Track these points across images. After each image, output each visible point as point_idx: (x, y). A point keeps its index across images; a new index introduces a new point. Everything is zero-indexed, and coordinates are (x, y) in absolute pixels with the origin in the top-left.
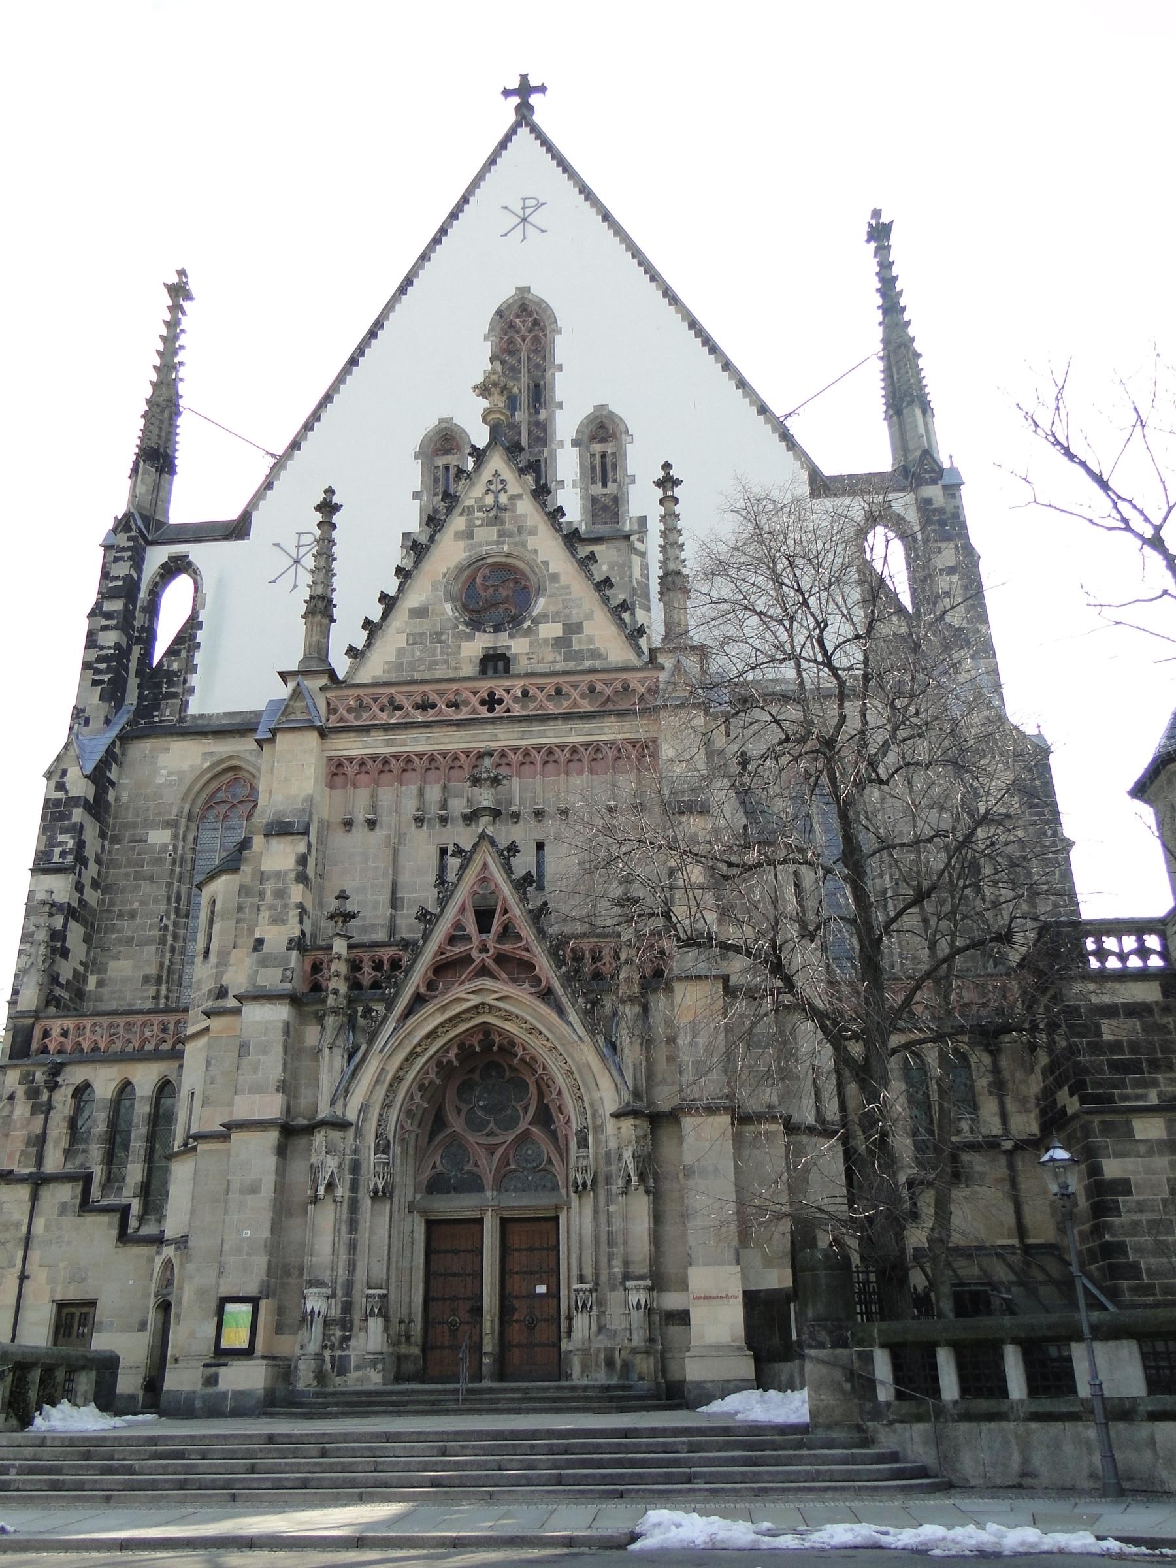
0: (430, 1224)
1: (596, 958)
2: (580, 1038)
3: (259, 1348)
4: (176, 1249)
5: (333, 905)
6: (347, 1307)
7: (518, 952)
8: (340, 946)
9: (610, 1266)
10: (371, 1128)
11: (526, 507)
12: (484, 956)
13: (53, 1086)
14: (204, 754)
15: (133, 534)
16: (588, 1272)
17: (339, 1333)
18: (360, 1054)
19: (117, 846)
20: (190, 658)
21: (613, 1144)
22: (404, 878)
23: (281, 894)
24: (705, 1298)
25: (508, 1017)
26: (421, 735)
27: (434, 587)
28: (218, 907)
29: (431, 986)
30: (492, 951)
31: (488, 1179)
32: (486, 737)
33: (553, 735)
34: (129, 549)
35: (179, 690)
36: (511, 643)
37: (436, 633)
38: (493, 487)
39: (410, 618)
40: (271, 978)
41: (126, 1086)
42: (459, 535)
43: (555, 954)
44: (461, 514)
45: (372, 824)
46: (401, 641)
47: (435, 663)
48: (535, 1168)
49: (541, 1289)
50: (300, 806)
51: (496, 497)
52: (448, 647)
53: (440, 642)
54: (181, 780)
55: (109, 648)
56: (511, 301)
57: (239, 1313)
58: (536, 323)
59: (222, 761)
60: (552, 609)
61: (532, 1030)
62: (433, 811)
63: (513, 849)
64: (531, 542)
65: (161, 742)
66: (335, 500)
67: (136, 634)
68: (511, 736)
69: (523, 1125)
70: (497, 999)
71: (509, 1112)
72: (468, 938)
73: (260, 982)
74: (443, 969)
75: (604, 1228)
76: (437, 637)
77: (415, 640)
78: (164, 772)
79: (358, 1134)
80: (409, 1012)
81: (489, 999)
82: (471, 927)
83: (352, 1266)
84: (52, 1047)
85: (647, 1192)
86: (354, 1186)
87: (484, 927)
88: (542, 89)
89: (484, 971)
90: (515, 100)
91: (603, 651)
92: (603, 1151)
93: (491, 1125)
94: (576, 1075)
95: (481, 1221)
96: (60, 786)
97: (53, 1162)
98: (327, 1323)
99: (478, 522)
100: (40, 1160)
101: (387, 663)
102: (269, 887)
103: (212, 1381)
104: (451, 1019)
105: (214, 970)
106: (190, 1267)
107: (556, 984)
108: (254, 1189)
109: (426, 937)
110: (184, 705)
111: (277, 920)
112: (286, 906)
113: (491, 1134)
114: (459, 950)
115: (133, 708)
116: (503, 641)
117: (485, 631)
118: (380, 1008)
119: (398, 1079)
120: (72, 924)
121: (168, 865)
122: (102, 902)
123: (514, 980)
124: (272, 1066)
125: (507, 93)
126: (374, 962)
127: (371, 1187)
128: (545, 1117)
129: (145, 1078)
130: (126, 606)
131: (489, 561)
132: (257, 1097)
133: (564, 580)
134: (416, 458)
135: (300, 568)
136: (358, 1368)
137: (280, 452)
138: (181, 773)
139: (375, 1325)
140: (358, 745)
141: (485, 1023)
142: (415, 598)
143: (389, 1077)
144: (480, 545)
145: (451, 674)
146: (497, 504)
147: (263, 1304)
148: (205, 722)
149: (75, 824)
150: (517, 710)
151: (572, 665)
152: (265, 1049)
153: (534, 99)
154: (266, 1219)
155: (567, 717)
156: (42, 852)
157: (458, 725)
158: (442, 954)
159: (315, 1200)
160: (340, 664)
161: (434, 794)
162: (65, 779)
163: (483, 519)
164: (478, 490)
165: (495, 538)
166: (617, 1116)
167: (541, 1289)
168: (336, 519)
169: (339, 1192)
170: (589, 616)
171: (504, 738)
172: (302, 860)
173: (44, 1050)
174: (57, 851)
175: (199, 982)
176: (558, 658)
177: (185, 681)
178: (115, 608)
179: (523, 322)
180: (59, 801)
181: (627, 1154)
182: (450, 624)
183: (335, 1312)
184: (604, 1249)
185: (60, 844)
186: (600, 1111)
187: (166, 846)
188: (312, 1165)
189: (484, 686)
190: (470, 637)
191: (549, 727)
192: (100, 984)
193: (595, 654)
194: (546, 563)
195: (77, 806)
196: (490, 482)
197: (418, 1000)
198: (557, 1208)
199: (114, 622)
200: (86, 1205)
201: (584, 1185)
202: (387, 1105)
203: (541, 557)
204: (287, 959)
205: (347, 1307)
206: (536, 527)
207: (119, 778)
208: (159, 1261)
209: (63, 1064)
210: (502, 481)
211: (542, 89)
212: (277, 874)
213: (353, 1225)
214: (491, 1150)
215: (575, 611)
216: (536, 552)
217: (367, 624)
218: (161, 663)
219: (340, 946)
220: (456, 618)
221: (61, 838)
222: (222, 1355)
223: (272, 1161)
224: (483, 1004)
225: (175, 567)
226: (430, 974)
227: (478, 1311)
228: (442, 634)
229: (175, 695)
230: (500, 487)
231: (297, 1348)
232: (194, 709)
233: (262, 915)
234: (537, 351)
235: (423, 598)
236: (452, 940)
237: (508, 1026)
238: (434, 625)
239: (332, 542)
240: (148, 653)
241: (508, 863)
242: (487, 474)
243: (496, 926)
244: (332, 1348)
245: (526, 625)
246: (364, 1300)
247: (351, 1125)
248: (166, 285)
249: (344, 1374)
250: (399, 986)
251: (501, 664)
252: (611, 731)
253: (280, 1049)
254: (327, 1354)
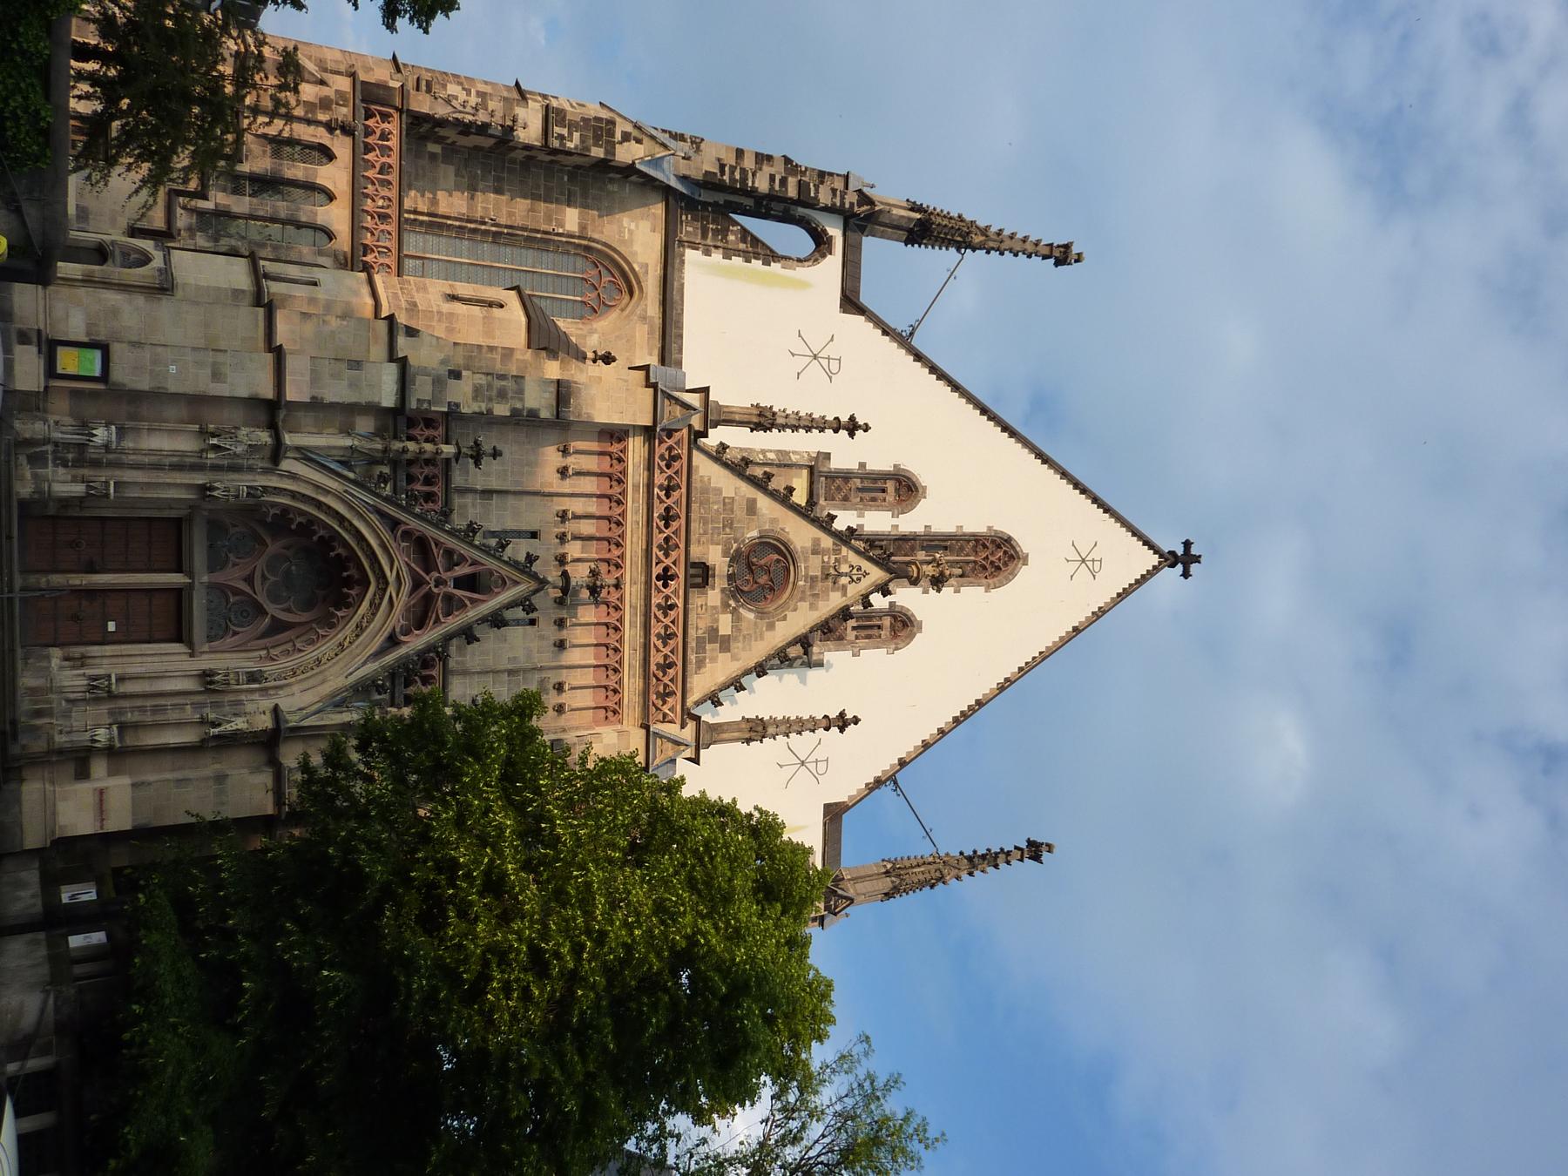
0: (178, 522)
1: (426, 680)
2: (351, 674)
4: (160, 270)
5: (487, 447)
7: (434, 615)
8: (448, 450)
9: (133, 709)
10: (273, 482)
11: (835, 601)
12: (432, 585)
13: (330, 127)
14: (647, 265)
15: (856, 208)
16: (129, 687)
17: (70, 456)
18: (346, 473)
19: (566, 178)
20: (738, 253)
21: (249, 707)
22: (511, 500)
24: (101, 800)
25: (375, 607)
26: (641, 517)
27: (774, 521)
28: (496, 311)
29: (407, 535)
30: (436, 590)
31: (220, 577)
32: (634, 574)
33: (631, 634)
34: (843, 203)
35: (709, 242)
36: (717, 590)
37: (732, 523)
38: (855, 571)
39: (748, 500)
40: (421, 391)
42: (816, 542)
43: (431, 648)
44: (834, 544)
45: (563, 472)
46: (728, 492)
48: (230, 621)
49: (111, 626)
50: (584, 411)
51: (846, 575)
52: (719, 534)
53: (724, 527)
54: (623, 242)
55: (753, 182)
56: (1018, 549)
57: (91, 363)
58: (998, 568)
59: (639, 283)
60: (744, 625)
61: (360, 629)
62: (571, 527)
63: (530, 609)
64: (804, 606)
65: (661, 225)
66: (859, 433)
67: (765, 203)
68: (633, 598)
69: (272, 609)
70: (391, 597)
71: (285, 594)
72: (449, 569)
73: (419, 379)
74: (422, 547)
75: (169, 701)
76: (729, 524)
77: (728, 504)
78: (633, 226)
79: (266, 471)
80: (382, 514)
81: (391, 589)
82: (462, 570)
84: (371, 122)
85: (203, 741)
86: (216, 468)
87: (460, 583)
88: (1186, 574)
89: (418, 583)
90: (1180, 551)
91: (703, 670)
92: (243, 697)
93: (272, 579)
94: (317, 670)
95: (179, 570)
96: (626, 137)
98: (81, 447)
99: (826, 559)
101: (709, 479)
103: (24, 338)
104: (373, 553)
105: (435, 309)
107: (403, 650)
108: (217, 376)
109: (452, 533)
110: (694, 246)
111: (477, 392)
112: (490, 399)
113: (264, 578)
114: (438, 561)
115: (697, 197)
116: (720, 582)
117: (730, 566)
118: (388, 490)
119: (319, 505)
120: (492, 141)
121: (544, 227)
122: (513, 161)
123: (408, 610)
124: (337, 392)
125: (1187, 544)
126: (433, 477)
127: (216, 485)
128: (278, 627)
129: (336, 216)
130: (791, 199)
131: (792, 568)
132: (307, 378)
133: (768, 635)
134: (895, 466)
135: (810, 359)
136: (35, 476)
137: (915, 342)
138: (631, 241)
139: (79, 489)
140: (637, 460)
141: (369, 583)
142: (764, 503)
143: (322, 499)
144: (806, 560)
145: (693, 538)
146: (841, 575)
147: (101, 387)
148: (677, 266)
149: (589, 150)
150: (656, 600)
151: (692, 644)
152: (353, 385)
153: (1180, 567)
154: (188, 388)
155: (646, 647)
156: (565, 116)
157: (647, 550)
158: (436, 545)
160: (715, 437)
161: (587, 528)
162: (633, 142)
163: (828, 563)
164: (853, 558)
165: (811, 574)
166: (276, 710)
167: (111, 626)
168: (843, 433)
169: (211, 455)
170: (734, 658)
171: (632, 593)
173: (369, 115)
174: (565, 132)
175: (425, 289)
176: (700, 632)
177: (716, 247)
178: (790, 189)
179: (999, 559)
180: (611, 134)
181: (239, 724)
182: (738, 535)
183: (92, 453)
184: (149, 703)
185: (570, 134)
186: (280, 692)
187: (563, 226)
188: (237, 428)
189: (680, 571)
190: (725, 554)
191: (639, 631)
192: (433, 156)
193: (700, 664)
194: (785, 618)
195: (607, 152)
196: (859, 569)
197: (394, 524)
198: (190, 645)
199: (777, 188)
201: (212, 683)
202: (294, 495)
203: (790, 614)
205: (96, 464)
206: (817, 610)
207: (631, 182)
209: (354, 135)
210: (859, 579)
211: (1186, 574)
213: (178, 467)
214: (249, 580)
215: (740, 645)
216: (795, 610)
218: (737, 224)
219: (448, 450)
220: (744, 540)
221: (576, 135)
223: (243, 392)
224: (387, 583)
225: (822, 243)
226: (417, 534)
227: (91, 569)
228: (731, 528)
229: (704, 236)
230: (855, 578)
231: (57, 418)
232: (691, 255)
233: (483, 377)
234: (974, 569)
235: (765, 511)
236: (449, 553)
237: (366, 604)
238: (739, 522)
239: (822, 430)
241: (517, 605)
242: (867, 566)
243: (459, 593)
244: (54, 452)
245: (732, 603)
246: (103, 479)
247: (277, 465)
248: (1072, 243)
249: (29, 462)
250: (407, 510)
251: (699, 580)
252: (631, 684)
253: (353, 399)
254: (49, 448)
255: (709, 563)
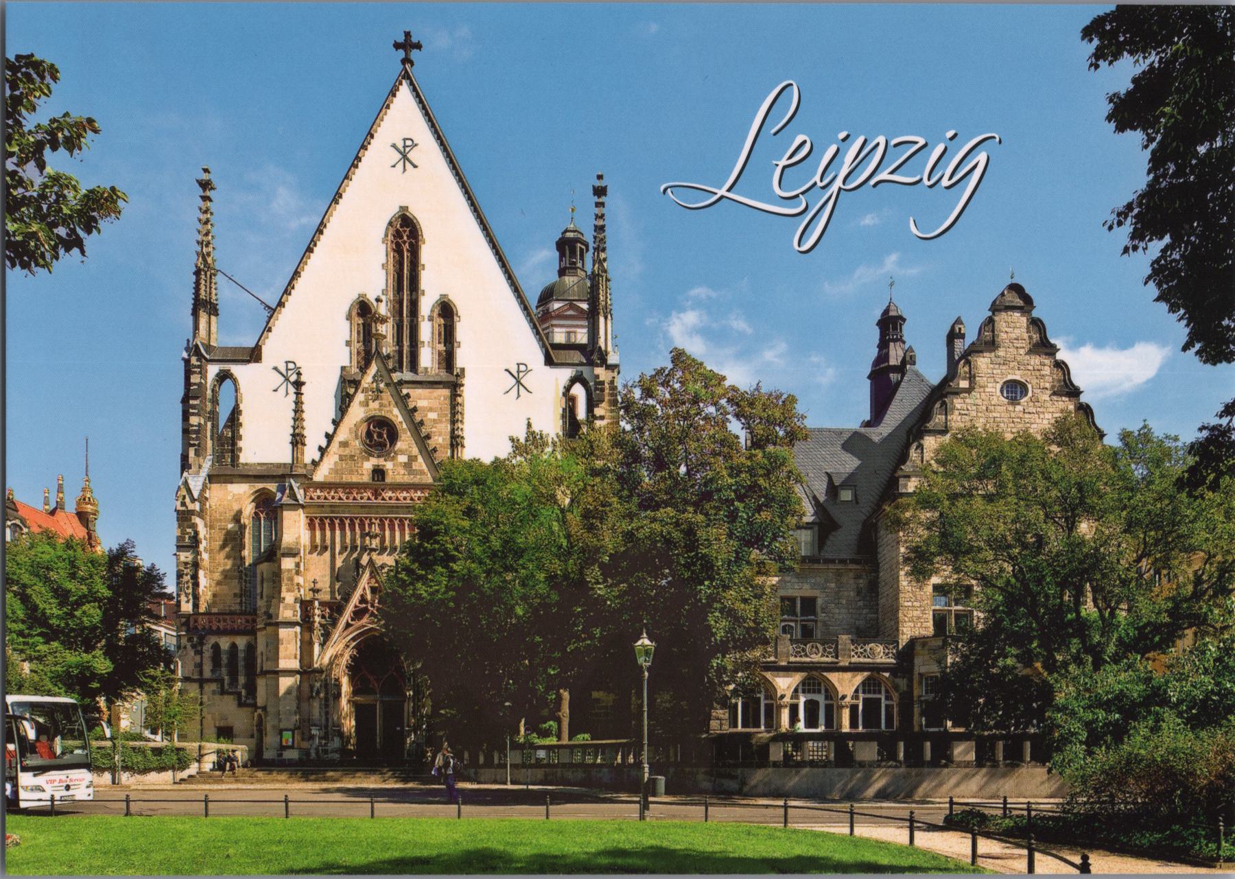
3: (296, 746)
6: (327, 733)
13: (201, 643)
23: (291, 579)
28: (265, 576)
41: (234, 646)
46: (336, 458)
47: (352, 471)
49: (398, 729)
51: (377, 384)
57: (287, 736)
76: (352, 457)
77: (341, 458)
83: (327, 720)
86: (327, 694)
97: (207, 673)
100: (201, 673)
102: (285, 576)
103: (281, 755)
106: (269, 718)
116: (381, 462)
129: (241, 642)
159: (312, 697)
167: (398, 729)
172: (298, 565)
197: (348, 625)
200: (223, 692)
204: (295, 607)
208: (256, 714)
212: (289, 571)
213: (327, 706)
217: (320, 448)
222: (283, 748)
240: (215, 426)
255: (371, 468)
